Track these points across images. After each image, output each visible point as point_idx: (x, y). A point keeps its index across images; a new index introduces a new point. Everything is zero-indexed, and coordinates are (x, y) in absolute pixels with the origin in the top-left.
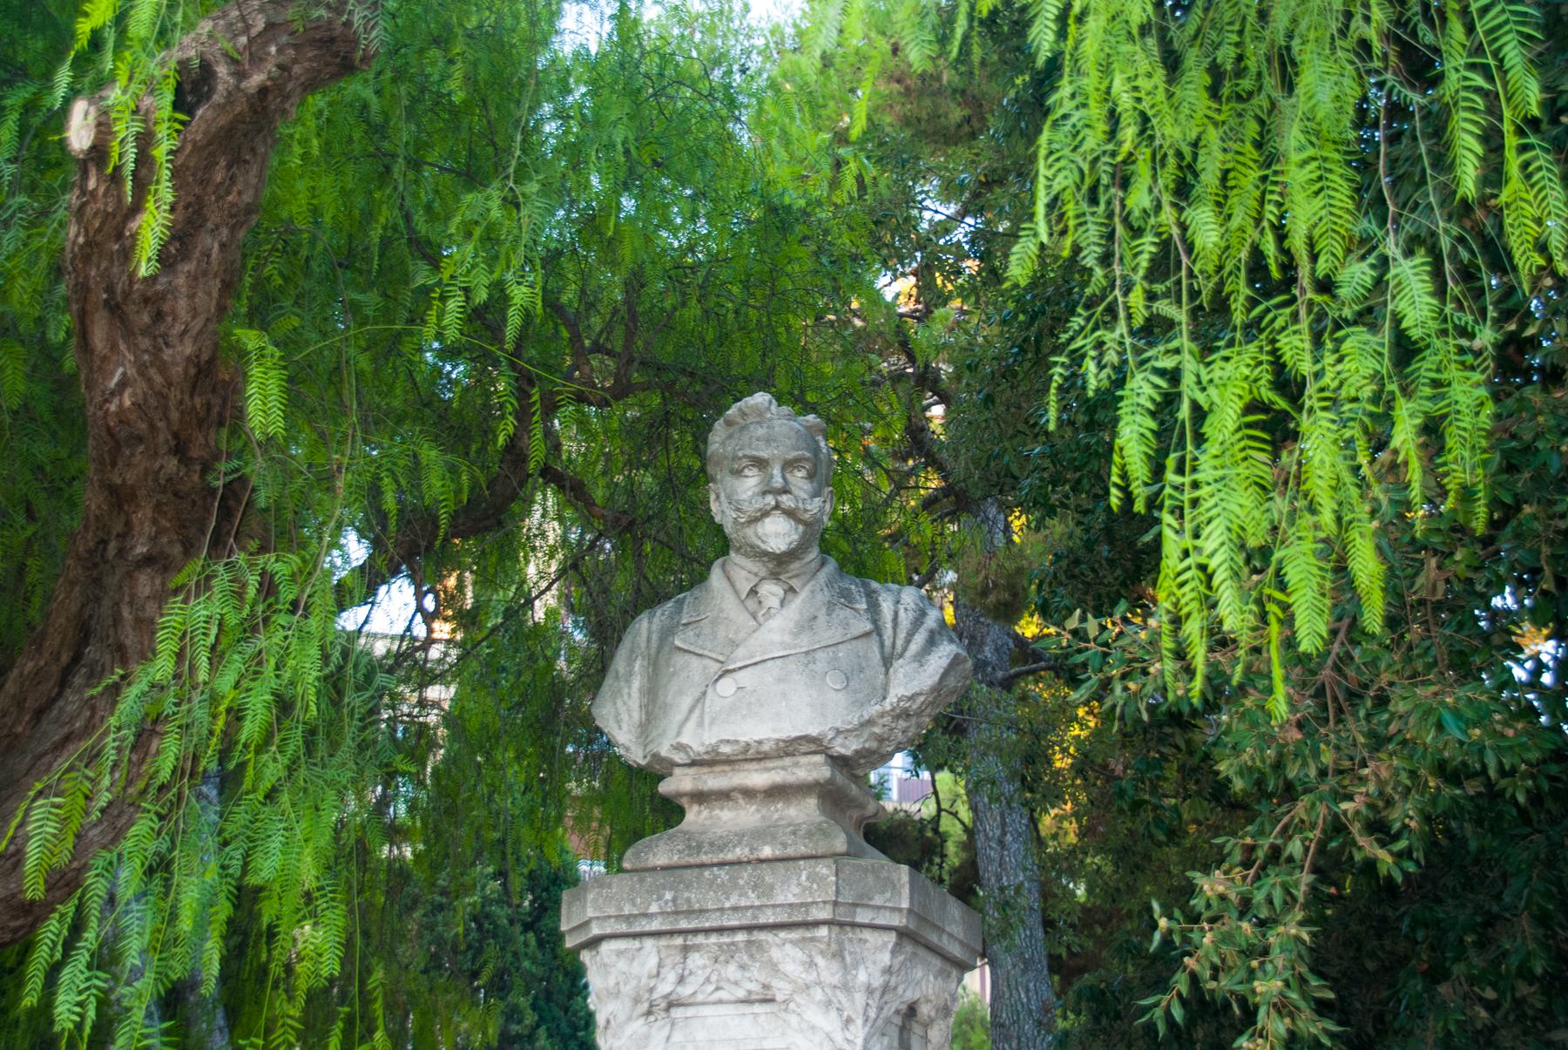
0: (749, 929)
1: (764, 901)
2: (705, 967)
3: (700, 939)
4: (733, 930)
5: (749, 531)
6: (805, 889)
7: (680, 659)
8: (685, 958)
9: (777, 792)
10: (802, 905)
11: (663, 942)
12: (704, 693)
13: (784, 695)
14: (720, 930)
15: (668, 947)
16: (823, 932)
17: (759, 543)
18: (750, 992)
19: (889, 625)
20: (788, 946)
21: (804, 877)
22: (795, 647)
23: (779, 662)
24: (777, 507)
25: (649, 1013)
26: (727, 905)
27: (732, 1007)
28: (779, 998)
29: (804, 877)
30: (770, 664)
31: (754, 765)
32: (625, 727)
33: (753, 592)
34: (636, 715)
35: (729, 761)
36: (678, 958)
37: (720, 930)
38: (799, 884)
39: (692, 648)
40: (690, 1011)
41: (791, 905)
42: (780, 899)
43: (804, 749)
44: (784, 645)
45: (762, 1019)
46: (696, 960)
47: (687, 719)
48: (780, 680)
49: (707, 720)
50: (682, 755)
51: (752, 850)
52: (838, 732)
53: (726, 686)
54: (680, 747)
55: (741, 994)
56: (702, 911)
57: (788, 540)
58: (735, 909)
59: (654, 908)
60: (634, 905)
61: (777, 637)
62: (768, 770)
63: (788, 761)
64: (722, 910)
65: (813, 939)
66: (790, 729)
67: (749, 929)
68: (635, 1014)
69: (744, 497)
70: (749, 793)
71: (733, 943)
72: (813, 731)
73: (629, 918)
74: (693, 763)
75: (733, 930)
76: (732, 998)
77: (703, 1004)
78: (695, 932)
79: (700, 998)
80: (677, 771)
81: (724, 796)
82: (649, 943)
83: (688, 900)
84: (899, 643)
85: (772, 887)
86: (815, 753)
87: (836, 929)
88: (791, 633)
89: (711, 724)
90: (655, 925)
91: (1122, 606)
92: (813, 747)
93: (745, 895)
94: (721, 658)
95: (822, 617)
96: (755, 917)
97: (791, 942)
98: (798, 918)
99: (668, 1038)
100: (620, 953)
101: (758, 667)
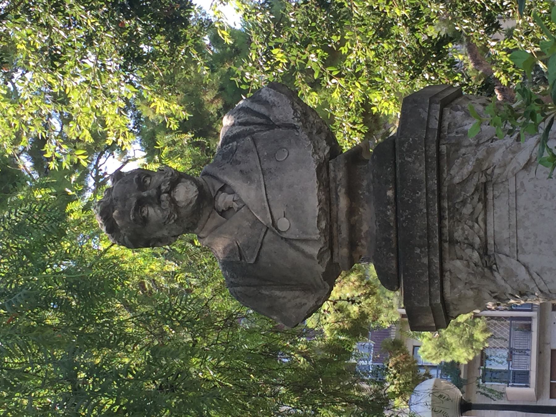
0: (440, 198)
1: (423, 185)
2: (463, 229)
3: (446, 231)
4: (440, 208)
5: (183, 212)
6: (416, 158)
7: (264, 259)
8: (457, 242)
9: (352, 194)
10: (426, 161)
11: (447, 256)
12: (286, 240)
13: (290, 186)
14: (441, 218)
15: (450, 253)
16: (444, 148)
17: (191, 205)
18: (480, 200)
19: (248, 128)
20: (452, 172)
21: (409, 159)
22: (259, 181)
23: (268, 192)
24: (169, 192)
25: (490, 268)
26: (425, 211)
27: (488, 214)
28: (483, 180)
29: (409, 159)
30: (270, 197)
31: (334, 208)
32: (304, 301)
33: (222, 213)
34: (297, 293)
35: (330, 226)
36: (457, 247)
37: (441, 218)
38: (414, 163)
39: (257, 251)
40: (491, 241)
41: (426, 168)
42: (423, 175)
43: (325, 175)
44: (259, 187)
45: (496, 193)
46: (458, 235)
47: (303, 252)
48: (281, 190)
49: (304, 237)
50: (325, 256)
51: (389, 203)
52: (315, 153)
53: (284, 224)
54: (321, 255)
55: (480, 206)
56: (428, 227)
57: (191, 186)
58: (428, 206)
59: (425, 261)
60: (423, 274)
61: (253, 194)
62: (337, 197)
63: (332, 185)
64: (428, 213)
65: (448, 155)
66: (314, 183)
67: (440, 198)
68: (492, 278)
69: (161, 215)
70: (352, 212)
71: (449, 209)
72: (314, 167)
73: (431, 277)
74: (331, 249)
75: (440, 208)
76: (483, 212)
77: (486, 233)
78: (441, 234)
79: (482, 233)
80: (336, 260)
81: (353, 228)
82: (448, 265)
83: (420, 237)
84: (260, 120)
85: (414, 180)
86: (328, 168)
87: (442, 141)
88: (250, 185)
89: (307, 234)
90: (436, 260)
91: (184, 115)
92: (324, 169)
93: (419, 200)
94: (264, 230)
95: (243, 167)
96: (433, 192)
97: (449, 170)
98: (435, 163)
99: (507, 256)
100: (453, 287)
101: (271, 204)
